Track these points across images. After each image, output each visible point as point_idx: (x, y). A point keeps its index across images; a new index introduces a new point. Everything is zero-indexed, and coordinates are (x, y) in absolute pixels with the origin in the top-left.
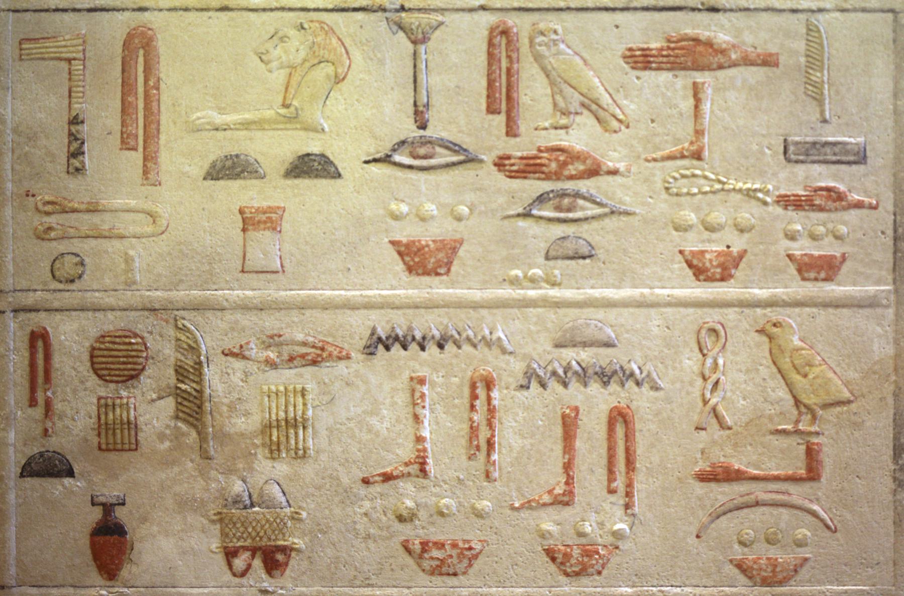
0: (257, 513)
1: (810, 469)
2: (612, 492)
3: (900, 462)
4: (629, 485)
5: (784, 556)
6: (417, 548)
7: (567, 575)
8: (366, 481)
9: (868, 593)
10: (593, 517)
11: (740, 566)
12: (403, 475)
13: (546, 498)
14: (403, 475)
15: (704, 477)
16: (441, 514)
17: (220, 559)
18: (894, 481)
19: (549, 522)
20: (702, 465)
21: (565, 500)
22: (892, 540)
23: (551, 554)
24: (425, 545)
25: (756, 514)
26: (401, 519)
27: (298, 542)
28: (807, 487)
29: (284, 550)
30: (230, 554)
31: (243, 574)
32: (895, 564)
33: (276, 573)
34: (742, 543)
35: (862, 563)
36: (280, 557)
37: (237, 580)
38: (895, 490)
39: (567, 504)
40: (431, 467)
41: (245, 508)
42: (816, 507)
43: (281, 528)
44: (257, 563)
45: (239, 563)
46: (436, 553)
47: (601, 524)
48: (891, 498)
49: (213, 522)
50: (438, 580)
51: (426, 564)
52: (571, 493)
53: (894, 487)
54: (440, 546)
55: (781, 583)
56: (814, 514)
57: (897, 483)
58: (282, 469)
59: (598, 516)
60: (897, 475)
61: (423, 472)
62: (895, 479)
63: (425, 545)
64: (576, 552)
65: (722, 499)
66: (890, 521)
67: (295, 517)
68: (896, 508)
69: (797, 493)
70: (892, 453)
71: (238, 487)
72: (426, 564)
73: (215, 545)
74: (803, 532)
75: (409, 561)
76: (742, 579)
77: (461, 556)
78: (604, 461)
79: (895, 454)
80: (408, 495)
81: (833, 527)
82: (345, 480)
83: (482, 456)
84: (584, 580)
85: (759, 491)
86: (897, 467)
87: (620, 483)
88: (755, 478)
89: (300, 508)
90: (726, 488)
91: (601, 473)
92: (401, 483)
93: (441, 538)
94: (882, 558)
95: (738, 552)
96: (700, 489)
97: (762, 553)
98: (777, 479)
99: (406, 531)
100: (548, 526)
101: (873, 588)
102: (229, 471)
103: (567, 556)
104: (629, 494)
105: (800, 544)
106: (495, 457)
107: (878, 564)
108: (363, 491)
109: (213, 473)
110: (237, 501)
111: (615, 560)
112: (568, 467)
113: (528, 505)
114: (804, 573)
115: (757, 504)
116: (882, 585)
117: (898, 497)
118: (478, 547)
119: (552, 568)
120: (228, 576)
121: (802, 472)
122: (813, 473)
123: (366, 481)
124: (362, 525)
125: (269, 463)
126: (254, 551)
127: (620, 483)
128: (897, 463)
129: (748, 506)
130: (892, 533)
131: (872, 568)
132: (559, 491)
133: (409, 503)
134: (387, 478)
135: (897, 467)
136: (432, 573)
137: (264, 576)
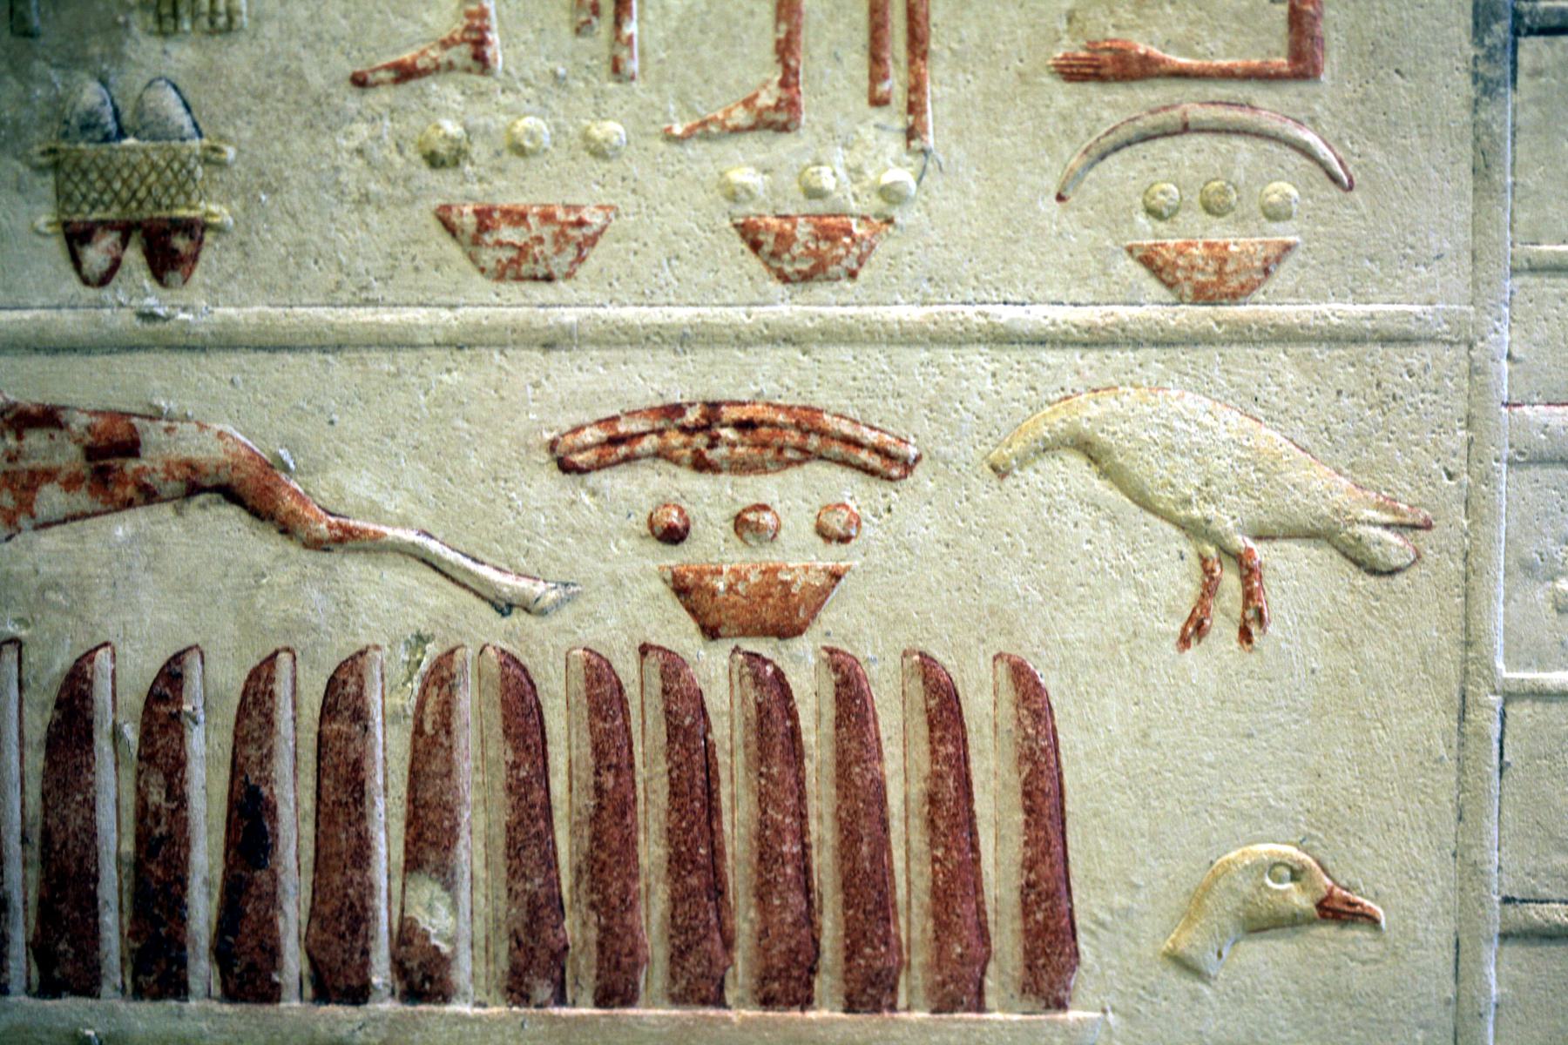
0: (132, 150)
1: (1297, 55)
2: (878, 102)
3: (1487, 41)
4: (916, 88)
5: (1241, 240)
6: (469, 221)
7: (784, 278)
8: (360, 82)
9: (1418, 319)
10: (839, 157)
11: (1148, 260)
12: (436, 69)
13: (740, 117)
14: (436, 69)
15: (1074, 72)
16: (519, 150)
17: (56, 247)
18: (1475, 82)
19: (746, 166)
20: (1069, 46)
21: (778, 120)
22: (1470, 208)
23: (750, 235)
24: (485, 218)
25: (1184, 151)
26: (434, 160)
27: (218, 211)
28: (1290, 94)
29: (191, 228)
30: (76, 237)
31: (104, 280)
32: (1474, 258)
33: (174, 277)
34: (1154, 213)
35: (1405, 256)
36: (181, 243)
37: (91, 293)
38: (1476, 102)
39: (784, 128)
40: (496, 49)
41: (107, 138)
42: (1308, 136)
43: (183, 184)
44: (134, 256)
45: (95, 256)
46: (508, 233)
47: (856, 172)
48: (1467, 117)
49: (39, 170)
50: (513, 290)
51: (488, 257)
52: (792, 105)
53: (1473, 94)
54: (517, 217)
55: (1234, 297)
56: (1306, 151)
57: (1481, 85)
58: (183, 55)
59: (847, 153)
60: (1481, 69)
61: (481, 60)
62: (1476, 78)
63: (485, 218)
64: (803, 231)
65: (1111, 118)
66: (1465, 166)
67: (211, 157)
68: (1478, 139)
69: (1269, 107)
70: (1470, 22)
71: (90, 95)
72: (488, 257)
73: (45, 218)
74: (1281, 189)
75: (452, 250)
76: (1153, 288)
77: (561, 239)
78: (862, 37)
79: (1476, 24)
80: (448, 110)
81: (1345, 179)
82: (317, 80)
83: (603, 27)
84: (821, 290)
85: (1191, 102)
86: (1481, 52)
87: (895, 84)
88: (1182, 74)
89: (221, 138)
90: (1119, 94)
91: (857, 62)
92: (433, 85)
93: (516, 200)
94: (1447, 245)
95: (1145, 231)
96: (1064, 96)
97: (1194, 234)
98: (1227, 75)
99: (445, 187)
100: (743, 175)
101: (1429, 308)
102: (73, 61)
103: (784, 239)
104: (914, 108)
105: (1274, 214)
106: (631, 28)
107: (1438, 257)
108: (353, 101)
109: (39, 66)
110: (89, 125)
111: (884, 248)
112: (785, 49)
113: (702, 131)
114: (1284, 276)
115: (1186, 128)
116: (1448, 302)
117: (1483, 115)
118: (596, 220)
119: (754, 264)
120: (72, 285)
121: (1281, 61)
122: (1303, 64)
123: (360, 82)
124: (352, 174)
125: (155, 44)
126: (126, 230)
127: (895, 84)
128: (1481, 43)
129: (1166, 133)
130: (1470, 193)
131: (1426, 265)
132: (766, 99)
133: (452, 128)
134: (405, 73)
135: (1481, 52)
136: (500, 277)
137: (148, 283)
